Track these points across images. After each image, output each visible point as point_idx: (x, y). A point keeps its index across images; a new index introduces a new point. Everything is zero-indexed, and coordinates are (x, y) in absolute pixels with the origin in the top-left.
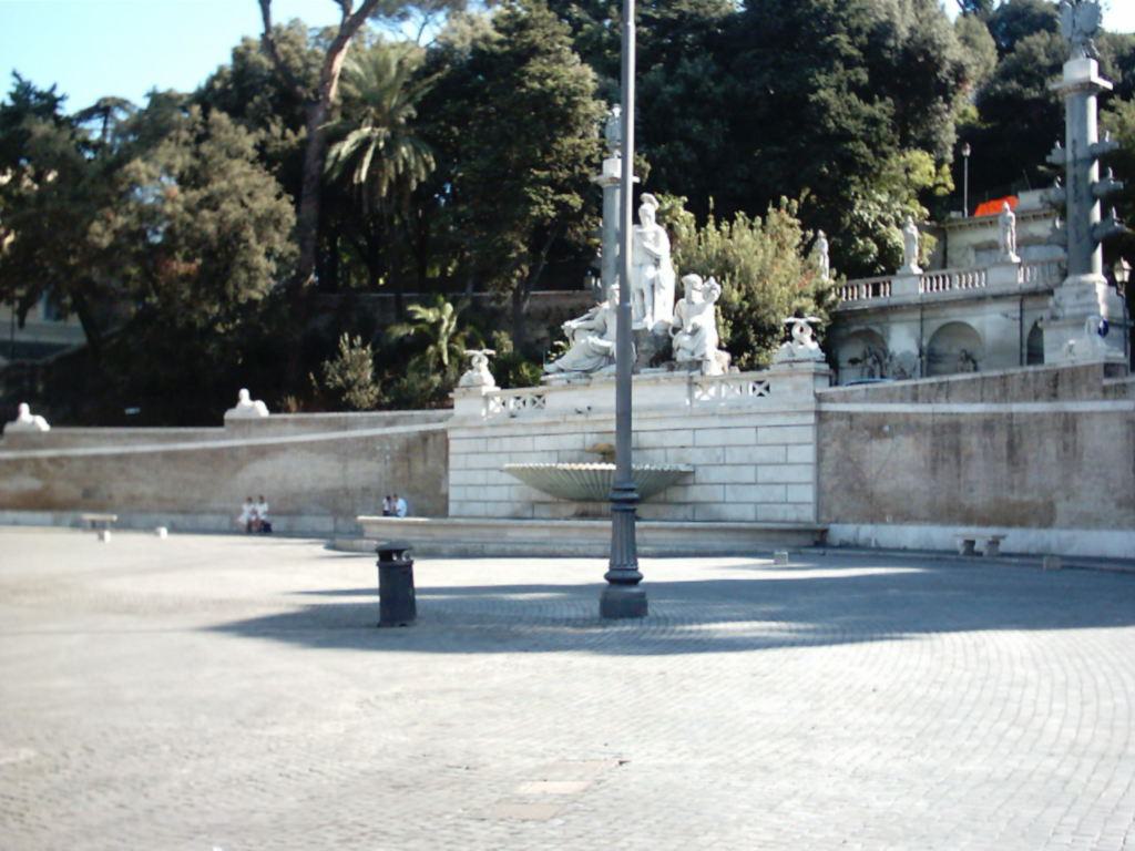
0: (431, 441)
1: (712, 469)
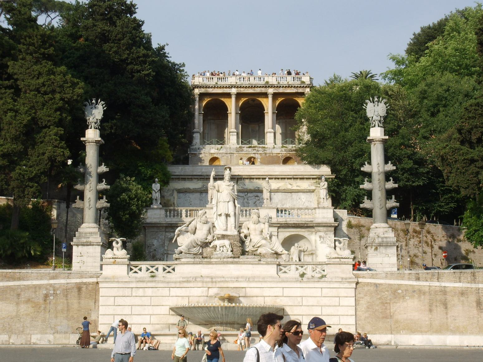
0: (84, 289)
1: (295, 308)
